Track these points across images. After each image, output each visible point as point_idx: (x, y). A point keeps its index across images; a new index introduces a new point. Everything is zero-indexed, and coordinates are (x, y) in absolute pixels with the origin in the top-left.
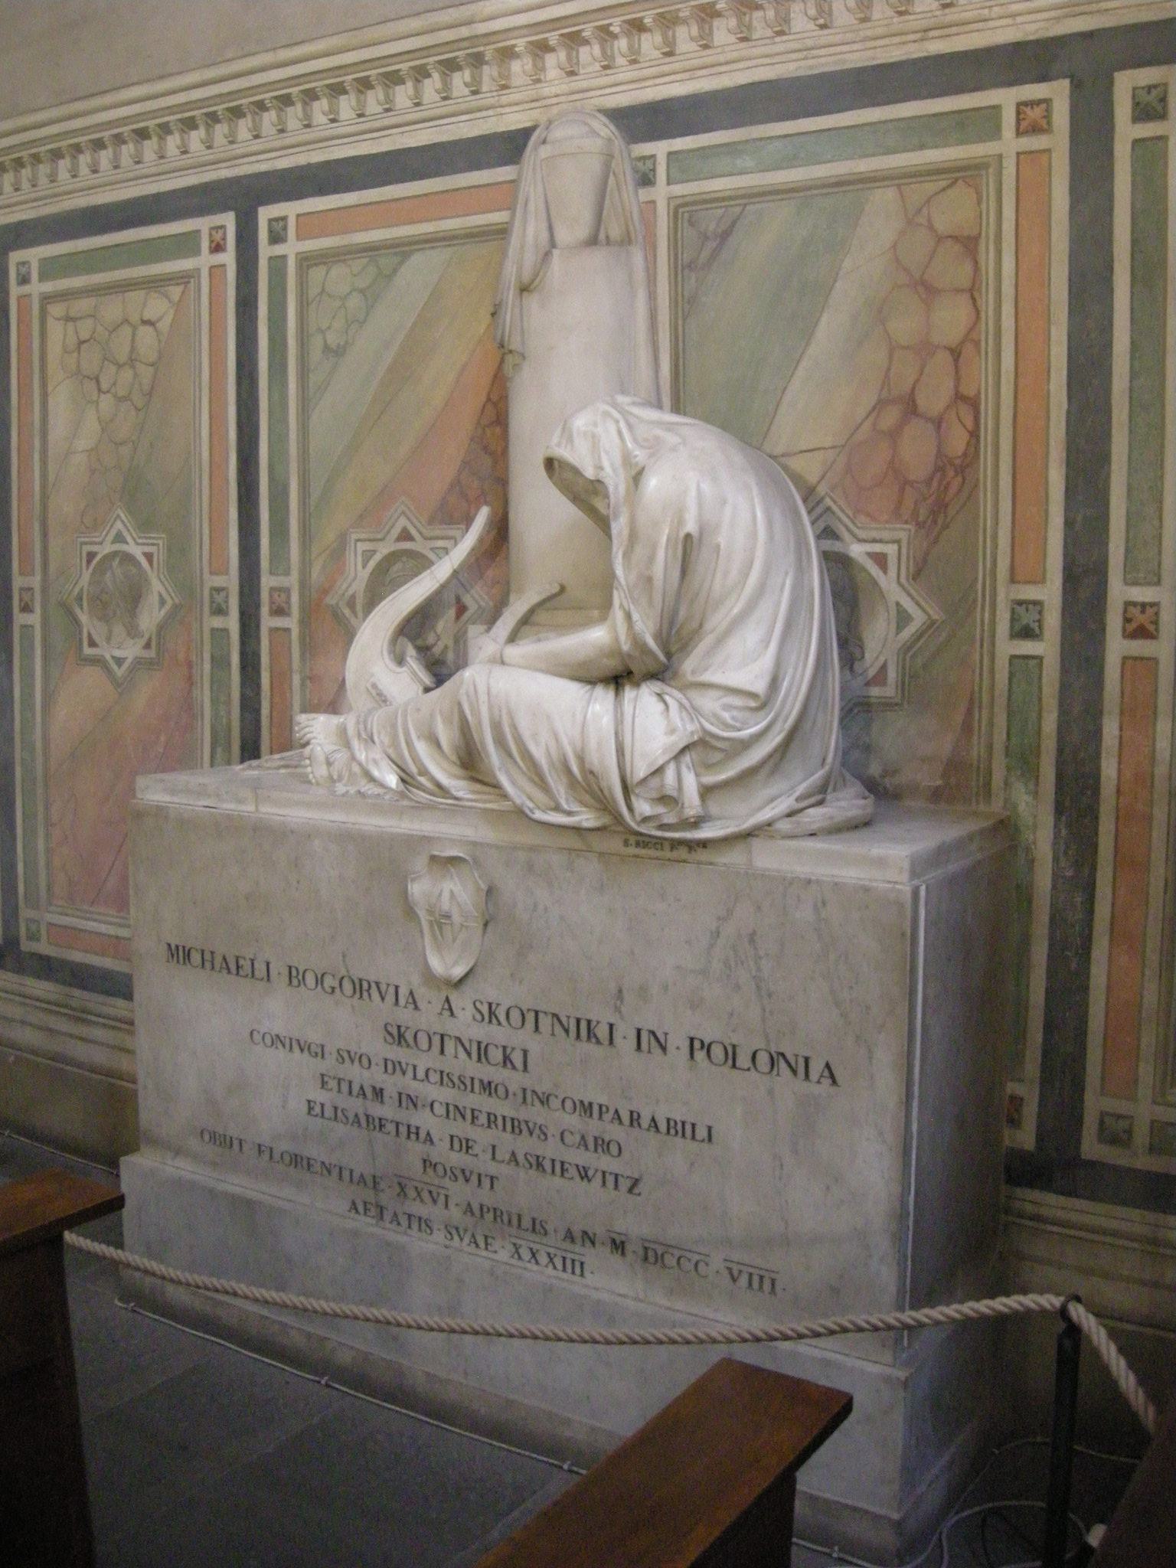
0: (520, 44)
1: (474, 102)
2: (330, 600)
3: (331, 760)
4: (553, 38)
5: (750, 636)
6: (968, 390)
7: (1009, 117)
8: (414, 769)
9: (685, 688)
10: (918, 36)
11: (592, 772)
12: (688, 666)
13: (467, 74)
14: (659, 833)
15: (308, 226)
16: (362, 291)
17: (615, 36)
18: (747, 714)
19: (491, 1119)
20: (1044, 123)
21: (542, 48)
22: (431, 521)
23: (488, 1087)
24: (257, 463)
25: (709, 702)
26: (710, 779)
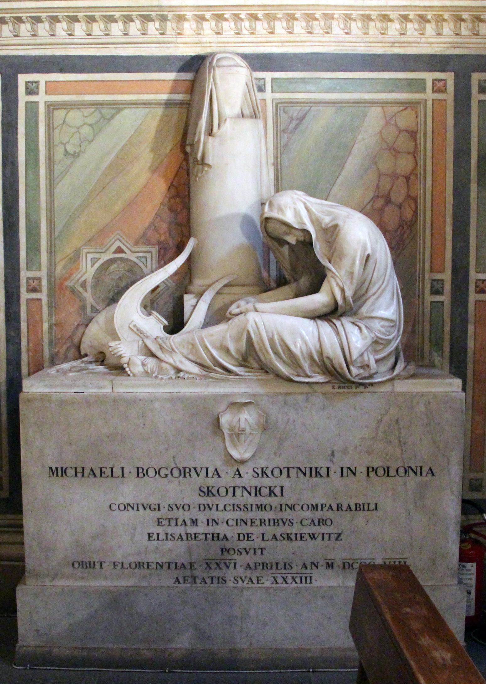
0: (189, 15)
1: (161, 38)
2: (69, 284)
3: (146, 363)
4: (208, 15)
5: (386, 298)
6: (413, 195)
7: (429, 85)
8: (209, 363)
9: (362, 318)
10: (390, 45)
11: (328, 358)
12: (364, 310)
13: (157, 24)
14: (361, 381)
15: (51, 88)
16: (91, 125)
17: (242, 20)
18: (389, 329)
19: (262, 522)
20: (443, 88)
21: (201, 19)
22: (136, 243)
23: (260, 507)
24: (18, 211)
25: (377, 325)
26: (379, 356)
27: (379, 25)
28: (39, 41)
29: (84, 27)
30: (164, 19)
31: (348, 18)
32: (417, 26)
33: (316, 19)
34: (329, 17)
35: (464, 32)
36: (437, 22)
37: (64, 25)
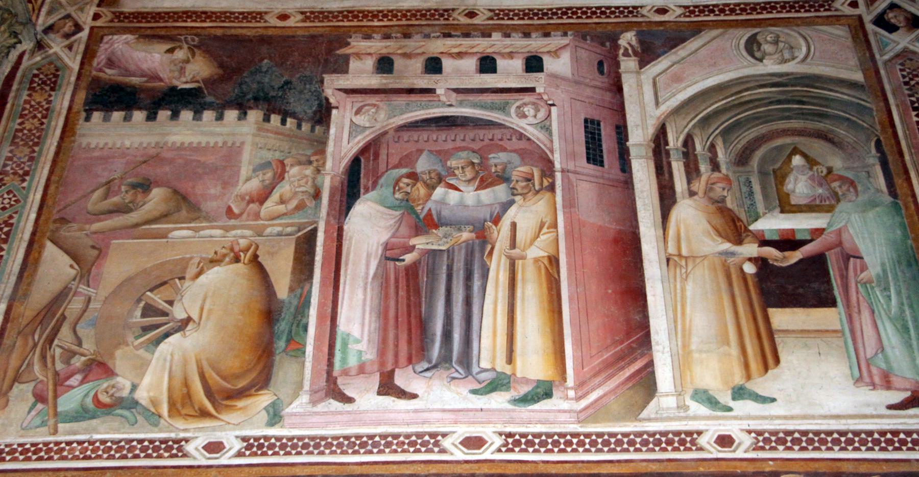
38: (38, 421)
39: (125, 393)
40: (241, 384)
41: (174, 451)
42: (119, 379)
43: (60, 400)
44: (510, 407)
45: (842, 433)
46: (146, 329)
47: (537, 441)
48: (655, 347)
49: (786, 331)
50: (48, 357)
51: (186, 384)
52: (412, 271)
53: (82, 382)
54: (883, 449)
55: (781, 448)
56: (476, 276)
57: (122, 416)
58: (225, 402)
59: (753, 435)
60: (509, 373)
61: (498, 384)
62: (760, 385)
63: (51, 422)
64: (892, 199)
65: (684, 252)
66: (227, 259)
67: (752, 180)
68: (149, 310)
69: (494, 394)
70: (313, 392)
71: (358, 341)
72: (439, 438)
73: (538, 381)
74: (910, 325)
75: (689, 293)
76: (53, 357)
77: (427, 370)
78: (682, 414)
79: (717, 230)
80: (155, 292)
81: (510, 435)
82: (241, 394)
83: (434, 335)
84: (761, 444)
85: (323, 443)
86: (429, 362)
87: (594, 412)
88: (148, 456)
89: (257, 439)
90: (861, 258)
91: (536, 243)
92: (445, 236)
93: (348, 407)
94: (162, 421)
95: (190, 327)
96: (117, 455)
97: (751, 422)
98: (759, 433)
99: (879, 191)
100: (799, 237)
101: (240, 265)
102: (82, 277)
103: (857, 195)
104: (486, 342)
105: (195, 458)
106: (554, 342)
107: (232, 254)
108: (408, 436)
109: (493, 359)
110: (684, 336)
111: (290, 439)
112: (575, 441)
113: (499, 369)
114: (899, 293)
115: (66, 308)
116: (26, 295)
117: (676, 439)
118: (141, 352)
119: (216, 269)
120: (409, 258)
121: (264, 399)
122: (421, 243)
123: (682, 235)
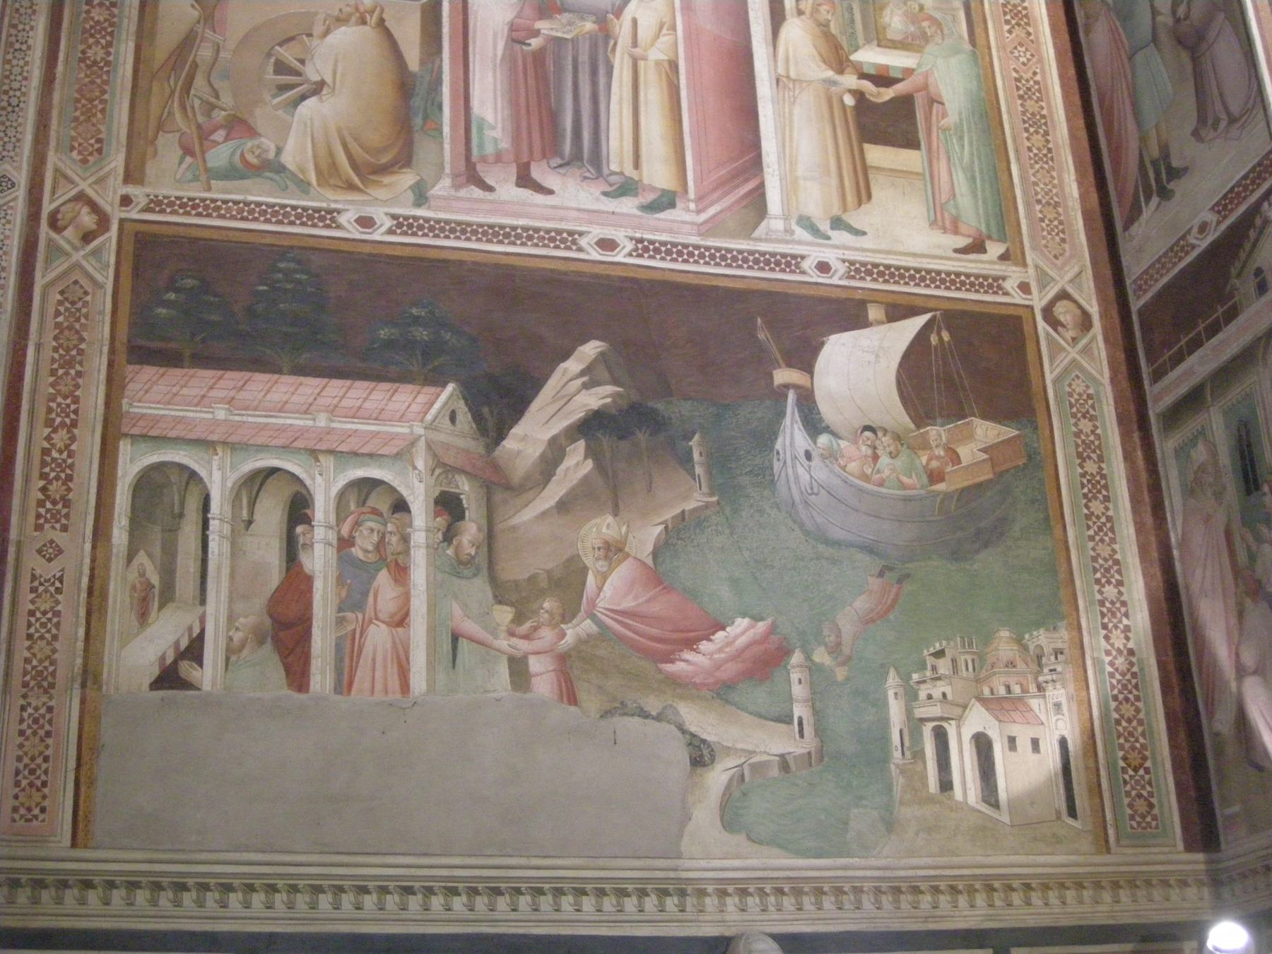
0: (710, 889)
1: (680, 916)
4: (730, 889)
17: (768, 895)
21: (723, 894)
27: (910, 898)
28: (541, 918)
29: (593, 902)
30: (682, 893)
31: (878, 891)
32: (948, 898)
33: (845, 893)
34: (858, 891)
35: (998, 903)
36: (969, 892)
37: (570, 898)
38: (189, 176)
39: (271, 155)
40: (385, 159)
41: (328, 222)
42: (263, 139)
43: (208, 156)
44: (639, 213)
45: (918, 270)
46: (283, 88)
47: (663, 249)
48: (766, 169)
49: (878, 168)
50: (188, 108)
51: (331, 154)
52: (539, 57)
53: (227, 139)
54: (948, 288)
55: (869, 278)
56: (602, 71)
57: (272, 179)
58: (371, 177)
59: (847, 264)
60: (636, 179)
61: (626, 188)
62: (855, 218)
63: (203, 178)
64: (971, 48)
65: (793, 75)
66: (353, 19)
67: (854, 7)
68: (281, 68)
69: (624, 199)
70: (455, 176)
71: (494, 128)
72: (576, 236)
73: (663, 190)
74: (978, 175)
75: (796, 119)
76: (193, 107)
77: (561, 166)
78: (788, 238)
79: (821, 55)
80: (284, 47)
81: (641, 241)
82: (384, 169)
83: (565, 130)
84: (853, 273)
85: (469, 229)
86: (562, 157)
87: (710, 228)
88: (303, 224)
89: (406, 218)
90: (942, 104)
91: (657, 44)
92: (570, 24)
93: (488, 195)
94: (312, 189)
95: (325, 91)
96: (274, 220)
97: (846, 252)
98: (852, 263)
99: (961, 37)
100: (893, 74)
101: (367, 28)
102: (206, 21)
103: (943, 39)
104: (614, 144)
105: (349, 231)
106: (676, 152)
107: (358, 15)
108: (548, 231)
109: (621, 163)
110: (791, 163)
111: (438, 221)
112: (696, 252)
113: (627, 174)
114: (971, 144)
115: (195, 56)
116: (152, 35)
117: (783, 261)
118: (280, 112)
119: (343, 29)
120: (535, 43)
121: (407, 179)
122: (544, 26)
123: (791, 57)
